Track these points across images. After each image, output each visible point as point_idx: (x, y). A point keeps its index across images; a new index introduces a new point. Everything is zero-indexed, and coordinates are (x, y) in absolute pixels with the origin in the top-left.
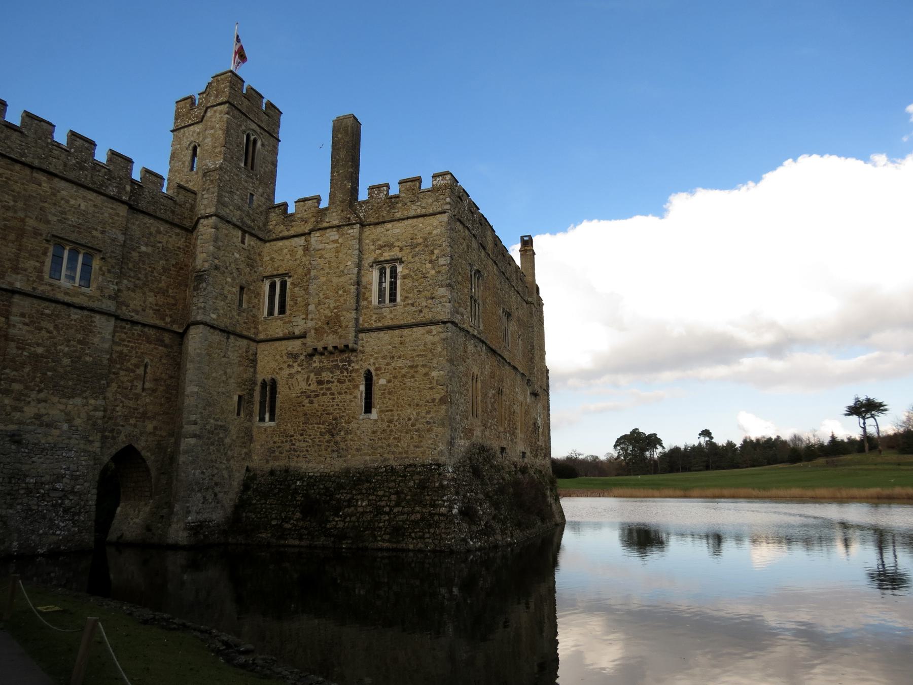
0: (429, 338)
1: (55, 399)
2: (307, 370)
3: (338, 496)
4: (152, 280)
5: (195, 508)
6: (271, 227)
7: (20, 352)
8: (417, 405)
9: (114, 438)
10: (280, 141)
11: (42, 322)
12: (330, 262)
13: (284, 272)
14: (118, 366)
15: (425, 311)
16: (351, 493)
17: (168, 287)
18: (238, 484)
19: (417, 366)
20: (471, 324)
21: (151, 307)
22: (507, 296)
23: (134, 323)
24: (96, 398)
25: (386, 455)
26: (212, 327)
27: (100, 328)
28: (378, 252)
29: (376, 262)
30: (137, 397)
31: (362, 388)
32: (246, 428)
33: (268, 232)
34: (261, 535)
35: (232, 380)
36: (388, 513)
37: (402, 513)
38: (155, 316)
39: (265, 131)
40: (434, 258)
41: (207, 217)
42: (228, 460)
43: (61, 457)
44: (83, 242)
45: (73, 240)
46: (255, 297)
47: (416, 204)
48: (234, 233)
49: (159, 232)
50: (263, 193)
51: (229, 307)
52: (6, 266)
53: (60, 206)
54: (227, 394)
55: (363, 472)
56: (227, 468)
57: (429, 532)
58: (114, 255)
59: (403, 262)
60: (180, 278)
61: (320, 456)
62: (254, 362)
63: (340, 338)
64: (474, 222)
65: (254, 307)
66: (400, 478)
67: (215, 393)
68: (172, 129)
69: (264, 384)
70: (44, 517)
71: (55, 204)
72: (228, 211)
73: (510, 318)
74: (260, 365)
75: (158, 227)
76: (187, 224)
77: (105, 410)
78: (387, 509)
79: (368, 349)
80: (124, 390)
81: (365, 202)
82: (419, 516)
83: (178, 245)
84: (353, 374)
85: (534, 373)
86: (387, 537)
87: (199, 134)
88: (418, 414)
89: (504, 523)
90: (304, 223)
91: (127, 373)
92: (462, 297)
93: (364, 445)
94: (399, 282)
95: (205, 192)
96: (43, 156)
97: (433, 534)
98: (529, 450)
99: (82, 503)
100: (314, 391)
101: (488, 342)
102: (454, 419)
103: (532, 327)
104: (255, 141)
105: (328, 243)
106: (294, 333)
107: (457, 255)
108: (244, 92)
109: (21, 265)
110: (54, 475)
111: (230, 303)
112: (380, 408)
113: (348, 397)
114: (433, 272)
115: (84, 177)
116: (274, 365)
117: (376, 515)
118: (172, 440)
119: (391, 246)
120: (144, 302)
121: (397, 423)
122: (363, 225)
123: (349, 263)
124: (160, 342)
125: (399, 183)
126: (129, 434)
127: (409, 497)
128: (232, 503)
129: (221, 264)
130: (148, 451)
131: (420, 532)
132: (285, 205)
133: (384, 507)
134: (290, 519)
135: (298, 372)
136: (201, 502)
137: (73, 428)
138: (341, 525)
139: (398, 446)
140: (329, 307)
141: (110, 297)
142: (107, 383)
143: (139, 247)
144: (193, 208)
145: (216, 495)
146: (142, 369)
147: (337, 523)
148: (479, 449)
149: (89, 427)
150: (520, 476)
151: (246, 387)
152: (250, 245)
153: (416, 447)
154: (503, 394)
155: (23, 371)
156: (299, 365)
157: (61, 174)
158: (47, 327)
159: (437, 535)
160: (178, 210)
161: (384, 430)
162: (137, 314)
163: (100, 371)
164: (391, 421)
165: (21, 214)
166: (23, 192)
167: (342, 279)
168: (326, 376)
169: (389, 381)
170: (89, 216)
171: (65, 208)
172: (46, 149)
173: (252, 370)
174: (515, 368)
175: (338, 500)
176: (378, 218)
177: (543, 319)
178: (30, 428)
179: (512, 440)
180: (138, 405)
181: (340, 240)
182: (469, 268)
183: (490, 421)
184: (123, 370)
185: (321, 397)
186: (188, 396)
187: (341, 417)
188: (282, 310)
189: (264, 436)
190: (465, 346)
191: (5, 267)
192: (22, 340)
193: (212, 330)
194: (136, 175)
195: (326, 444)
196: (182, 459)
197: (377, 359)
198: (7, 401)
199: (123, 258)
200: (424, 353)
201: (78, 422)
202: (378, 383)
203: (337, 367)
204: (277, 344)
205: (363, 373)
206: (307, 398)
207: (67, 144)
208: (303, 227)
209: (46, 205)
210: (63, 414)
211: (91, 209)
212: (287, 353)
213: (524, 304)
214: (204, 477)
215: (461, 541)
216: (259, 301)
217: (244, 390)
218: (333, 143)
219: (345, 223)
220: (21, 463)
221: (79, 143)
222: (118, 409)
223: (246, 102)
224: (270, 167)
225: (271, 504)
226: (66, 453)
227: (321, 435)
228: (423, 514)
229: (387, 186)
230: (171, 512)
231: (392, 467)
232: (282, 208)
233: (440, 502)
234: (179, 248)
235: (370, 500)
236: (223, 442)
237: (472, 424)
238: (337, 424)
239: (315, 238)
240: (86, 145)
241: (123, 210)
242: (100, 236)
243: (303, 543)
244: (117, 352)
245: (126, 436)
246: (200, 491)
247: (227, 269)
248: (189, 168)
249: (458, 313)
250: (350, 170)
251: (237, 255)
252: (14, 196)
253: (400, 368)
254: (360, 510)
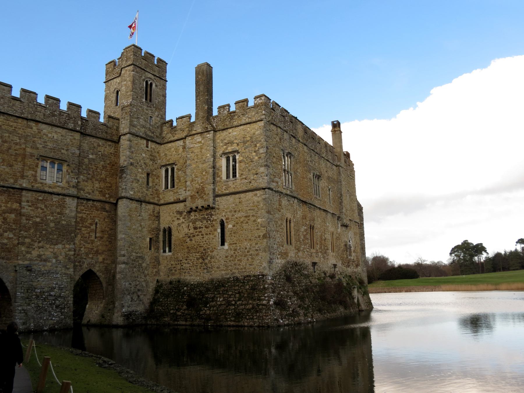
0: (256, 199)
1: (48, 246)
2: (188, 221)
3: (207, 296)
4: (97, 174)
5: (126, 304)
6: (164, 135)
7: (28, 221)
8: (250, 240)
9: (80, 266)
10: (167, 81)
11: (38, 204)
12: (197, 155)
13: (173, 162)
14: (81, 225)
15: (253, 182)
16: (214, 294)
17: (106, 177)
18: (152, 290)
19: (249, 216)
20: (284, 187)
21: (97, 190)
22: (317, 164)
23: (88, 200)
24: (69, 244)
25: (233, 271)
26: (131, 199)
27: (69, 204)
28: (225, 147)
29: (224, 154)
30: (92, 242)
31: (219, 230)
32: (156, 257)
33: (162, 138)
34: (165, 319)
35: (145, 229)
36: (234, 305)
37: (242, 305)
38: (99, 195)
39: (157, 77)
40: (257, 149)
41: (125, 135)
42: (145, 276)
43: (52, 277)
44: (57, 157)
45: (51, 157)
46: (157, 178)
47: (245, 116)
48: (141, 142)
49: (99, 146)
50: (158, 115)
51: (141, 186)
52: (18, 175)
53: (43, 139)
54: (143, 238)
55: (221, 281)
56: (145, 281)
57: (256, 316)
58: (74, 162)
59: (239, 153)
60: (113, 171)
61: (197, 272)
62: (158, 217)
63: (205, 201)
64: (285, 122)
65: (156, 184)
66: (241, 284)
67: (135, 238)
68: (105, 81)
69: (165, 230)
70: (46, 310)
71: (40, 138)
72: (137, 129)
73: (320, 179)
74: (161, 218)
75: (98, 143)
76: (115, 138)
77: (75, 251)
78: (233, 302)
79: (221, 207)
80: (85, 239)
81: (216, 116)
82: (251, 306)
83: (111, 152)
84: (214, 223)
85: (343, 212)
86: (233, 319)
87: (119, 83)
88: (251, 245)
89: (307, 309)
90: (182, 131)
91: (86, 229)
92: (276, 171)
93: (221, 264)
94: (237, 165)
95: (123, 120)
96: (32, 112)
97: (258, 316)
98: (341, 262)
99: (66, 302)
100: (192, 233)
101: (299, 197)
102: (272, 247)
103: (341, 182)
104: (151, 84)
105: (196, 144)
106: (180, 199)
107: (271, 146)
108: (143, 55)
109: (25, 174)
110: (50, 287)
111: (141, 184)
112: (230, 242)
113: (211, 236)
114: (257, 158)
115: (55, 120)
116: (169, 218)
117: (227, 307)
118: (114, 266)
119: (231, 143)
120: (93, 187)
121: (239, 251)
122: (215, 131)
123: (208, 155)
124: (104, 209)
125: (235, 104)
126: (89, 263)
127: (246, 295)
128: (149, 301)
129: (134, 162)
130: (100, 273)
131: (251, 315)
132: (171, 121)
133: (232, 301)
134: (180, 309)
135: (183, 222)
136: (130, 301)
137: (58, 261)
138: (208, 312)
139: (240, 265)
140: (198, 183)
141: (73, 187)
142: (75, 235)
143: (88, 156)
144: (118, 128)
145: (139, 296)
146: (94, 226)
147: (206, 311)
148: (292, 264)
149: (67, 260)
150: (328, 280)
151: (154, 233)
152: (151, 148)
153: (250, 265)
154: (314, 228)
155: (30, 232)
156: (183, 218)
157: (42, 121)
158: (41, 207)
159: (260, 317)
160: (109, 131)
161: (232, 256)
162: (90, 195)
163: (71, 229)
164: (235, 250)
165: (23, 146)
166: (24, 134)
167: (205, 165)
168: (198, 224)
169: (234, 226)
170: (59, 142)
171: (46, 140)
172: (34, 108)
173: (157, 222)
174: (327, 211)
175: (207, 298)
176: (224, 126)
177: (354, 174)
178: (36, 262)
179: (324, 257)
180: (93, 246)
181: (203, 142)
182: (282, 153)
183: (303, 246)
184: (84, 227)
185: (196, 237)
186: (119, 241)
187: (208, 248)
188: (173, 186)
189: (166, 261)
190: (280, 201)
191: (17, 176)
192: (28, 215)
193: (131, 201)
194: (84, 114)
195: (200, 265)
196: (118, 276)
197: (226, 213)
198: (23, 249)
199: (79, 163)
200: (253, 208)
201: (60, 258)
202: (227, 227)
203: (204, 218)
204: (171, 206)
205: (219, 222)
206: (188, 238)
207: (45, 103)
208: (181, 134)
209: (35, 139)
210: (52, 254)
211: (60, 138)
212: (176, 211)
213: (334, 167)
214: (131, 286)
215: (274, 320)
216: (159, 180)
217: (153, 234)
218: (196, 81)
219: (205, 131)
220: (33, 282)
221: (51, 101)
222: (82, 249)
223: (144, 62)
224: (162, 98)
225: (170, 301)
226: (55, 275)
227: (197, 259)
228: (253, 305)
229: (229, 106)
230: (114, 307)
231: (237, 278)
232: (170, 123)
233: (263, 298)
234: (111, 153)
235: (224, 297)
236: (141, 265)
237: (287, 249)
238: (206, 253)
239: (188, 140)
240: (55, 102)
241: (77, 136)
242: (66, 152)
243: (188, 323)
244: (79, 217)
245: (87, 264)
246: (129, 294)
247: (138, 164)
248: (115, 104)
249: (273, 182)
250: (207, 97)
251: (144, 155)
252: (19, 137)
253: (240, 218)
254: (219, 303)
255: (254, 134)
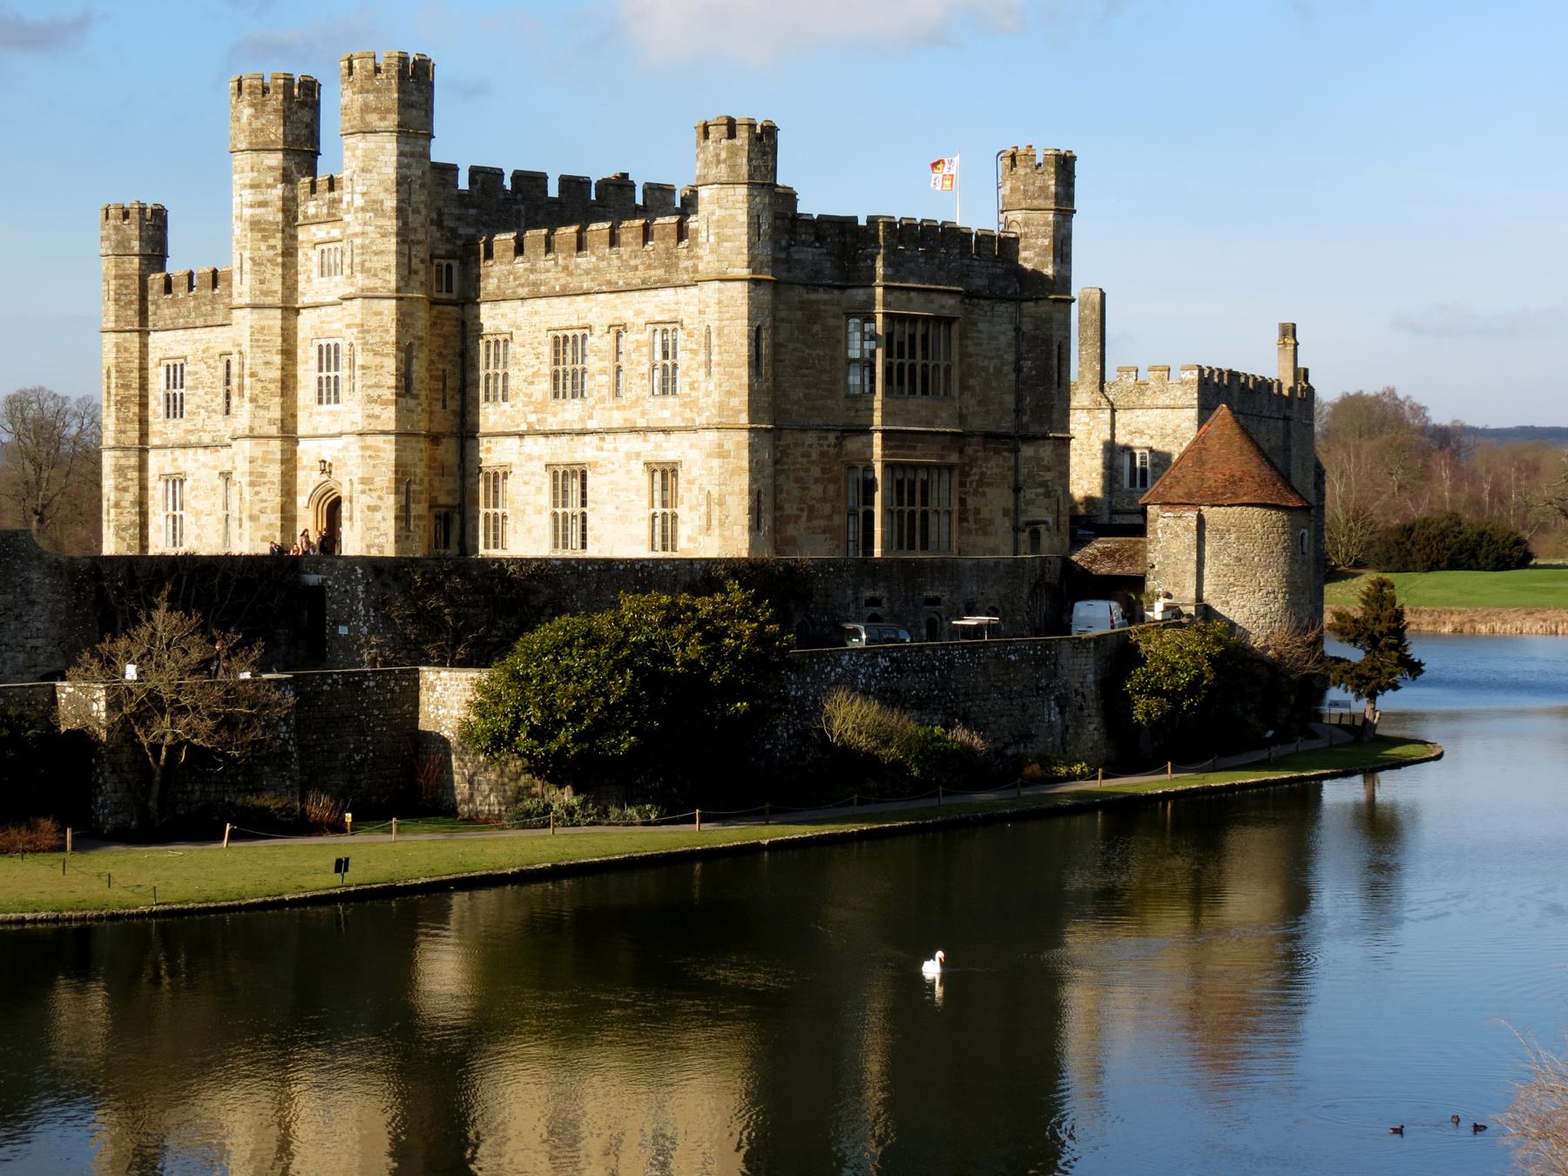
119: (1142, 433)
140: (1082, 488)
181: (1092, 423)
255: (1179, 426)
